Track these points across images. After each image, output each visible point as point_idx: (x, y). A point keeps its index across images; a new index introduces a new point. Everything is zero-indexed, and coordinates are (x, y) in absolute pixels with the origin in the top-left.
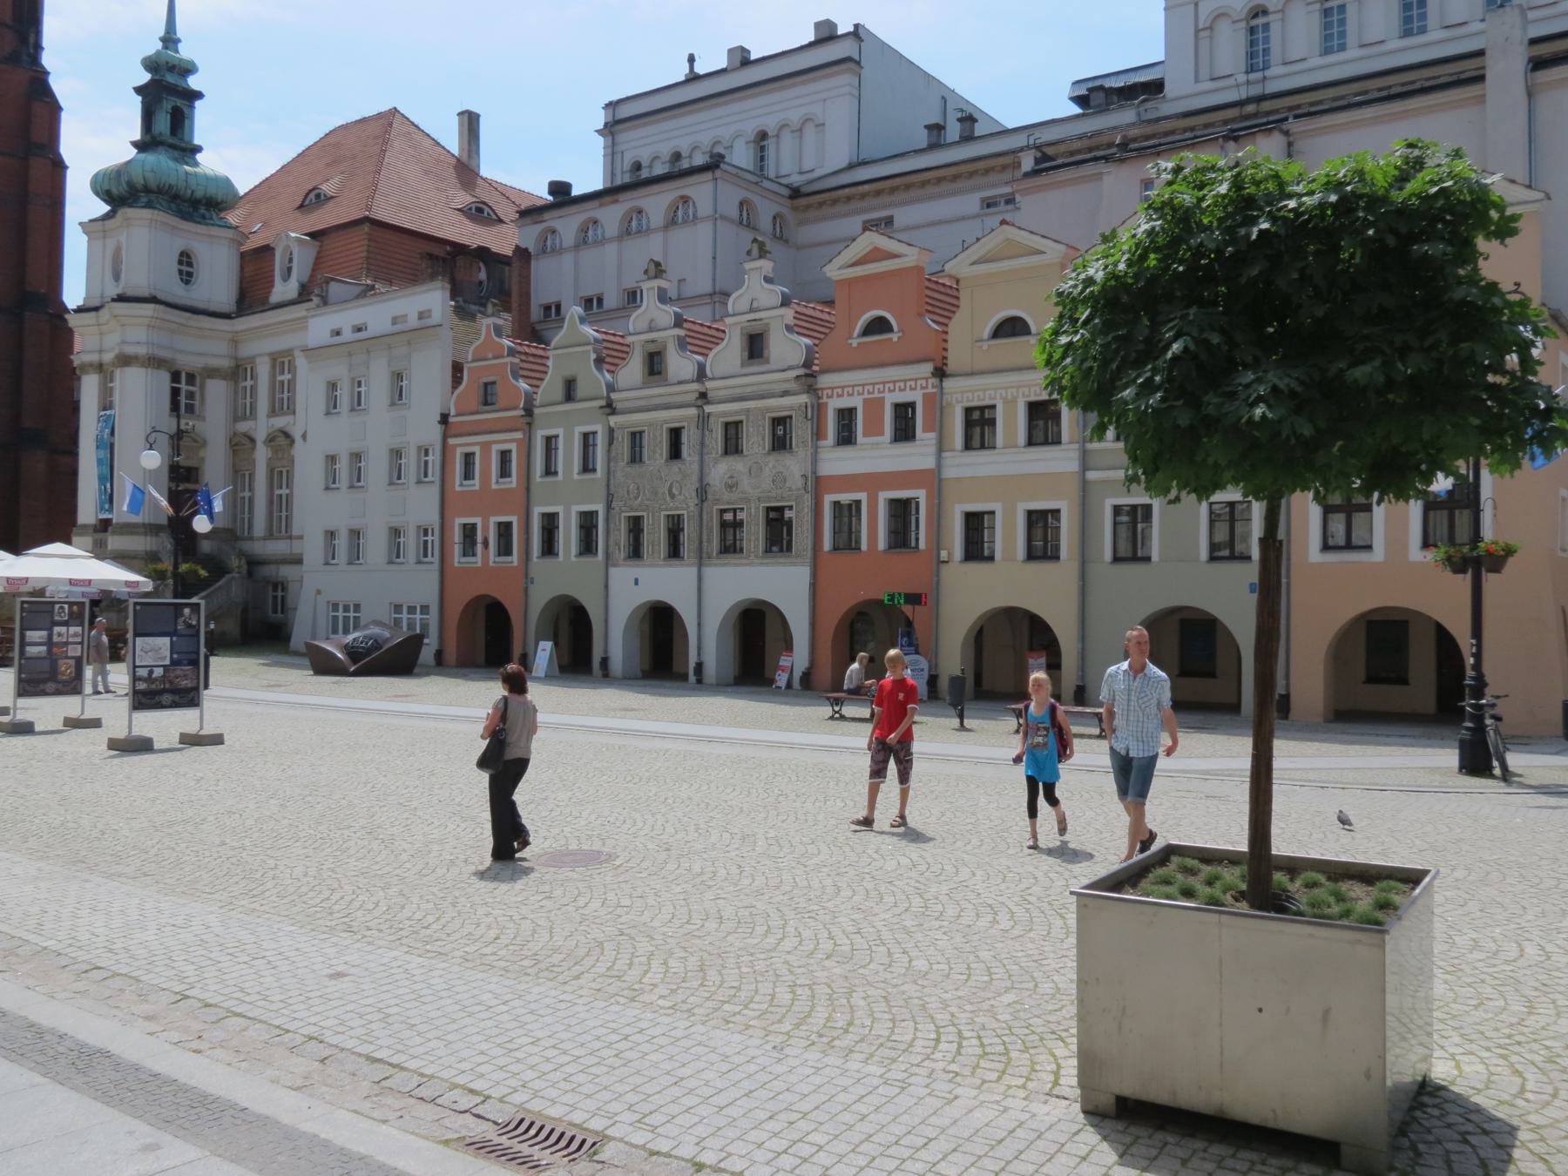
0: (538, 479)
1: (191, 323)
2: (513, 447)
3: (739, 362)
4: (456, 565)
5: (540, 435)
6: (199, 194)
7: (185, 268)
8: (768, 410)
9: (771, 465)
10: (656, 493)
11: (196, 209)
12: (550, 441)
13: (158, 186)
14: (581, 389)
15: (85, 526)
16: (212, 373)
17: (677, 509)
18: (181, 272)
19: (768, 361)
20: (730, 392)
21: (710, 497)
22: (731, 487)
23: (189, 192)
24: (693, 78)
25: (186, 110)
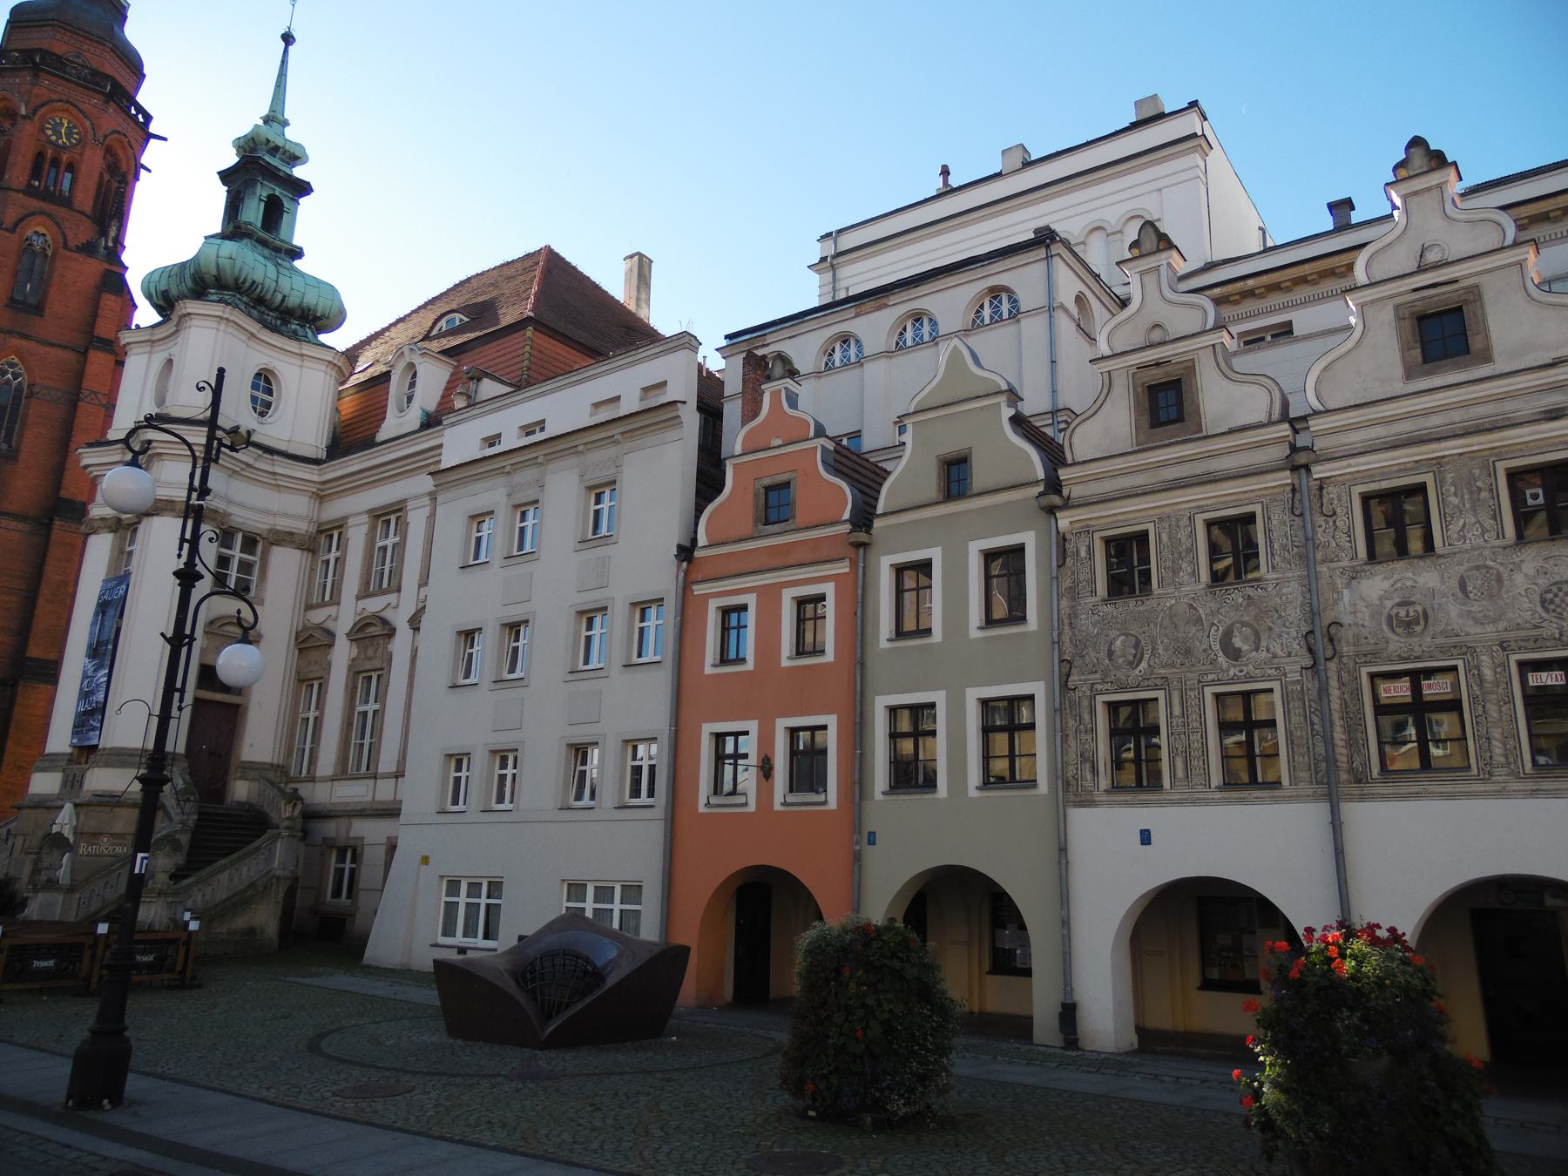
0: (884, 644)
1: (259, 465)
3: (1399, 371)
4: (702, 809)
6: (293, 301)
7: (261, 395)
8: (1499, 453)
9: (1529, 568)
10: (1188, 652)
11: (285, 322)
13: (236, 280)
14: (980, 476)
15: (56, 757)
16: (281, 538)
17: (1250, 678)
18: (254, 399)
19: (1486, 357)
20: (1381, 431)
21: (1346, 649)
22: (1408, 625)
23: (279, 297)
24: (948, 192)
25: (287, 204)
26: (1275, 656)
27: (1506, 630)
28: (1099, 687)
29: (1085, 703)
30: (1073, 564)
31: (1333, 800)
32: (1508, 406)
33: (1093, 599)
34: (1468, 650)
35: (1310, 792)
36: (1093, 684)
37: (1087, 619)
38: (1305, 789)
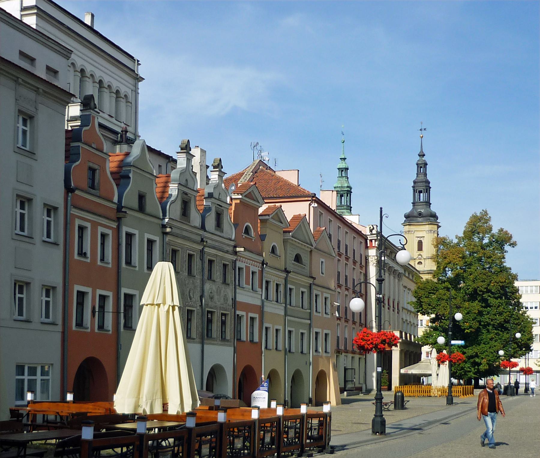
2: (109, 232)
5: (125, 229)
12: (129, 236)
14: (149, 208)
26: (196, 301)
27: (221, 304)
31: (203, 344)
32: (224, 246)
34: (216, 307)
35: (198, 341)
38: (198, 340)
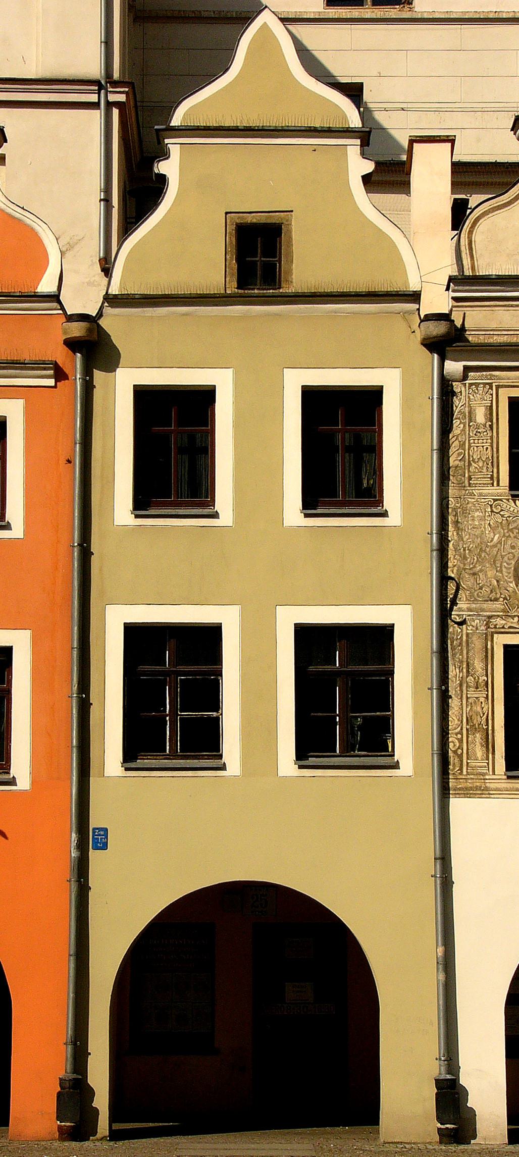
28: (500, 622)
29: (477, 643)
30: (463, 430)
33: (494, 490)
36: (490, 617)
37: (483, 519)
